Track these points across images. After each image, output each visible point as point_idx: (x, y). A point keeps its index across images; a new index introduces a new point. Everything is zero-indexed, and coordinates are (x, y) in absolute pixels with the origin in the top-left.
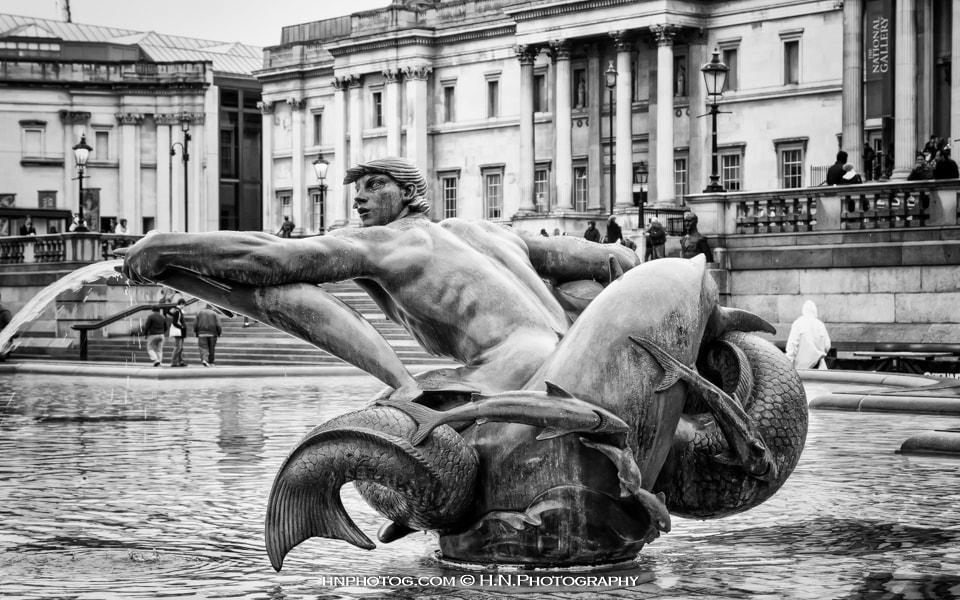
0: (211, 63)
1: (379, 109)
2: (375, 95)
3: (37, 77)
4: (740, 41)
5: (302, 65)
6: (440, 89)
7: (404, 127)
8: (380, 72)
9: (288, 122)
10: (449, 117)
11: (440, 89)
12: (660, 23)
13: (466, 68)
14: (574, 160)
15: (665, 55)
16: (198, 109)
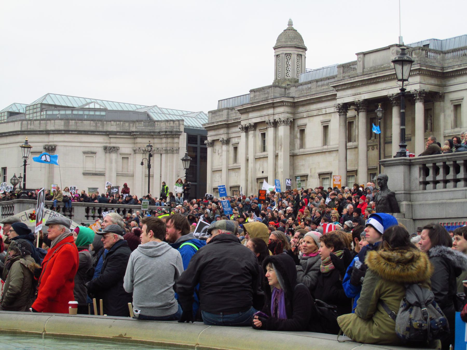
0: (183, 120)
1: (264, 142)
2: (262, 134)
3: (92, 129)
4: (463, 99)
5: (227, 121)
6: (297, 130)
7: (277, 152)
8: (265, 121)
9: (220, 151)
10: (302, 146)
11: (297, 130)
12: (416, 89)
13: (311, 118)
14: (368, 169)
15: (419, 107)
16: (175, 145)
